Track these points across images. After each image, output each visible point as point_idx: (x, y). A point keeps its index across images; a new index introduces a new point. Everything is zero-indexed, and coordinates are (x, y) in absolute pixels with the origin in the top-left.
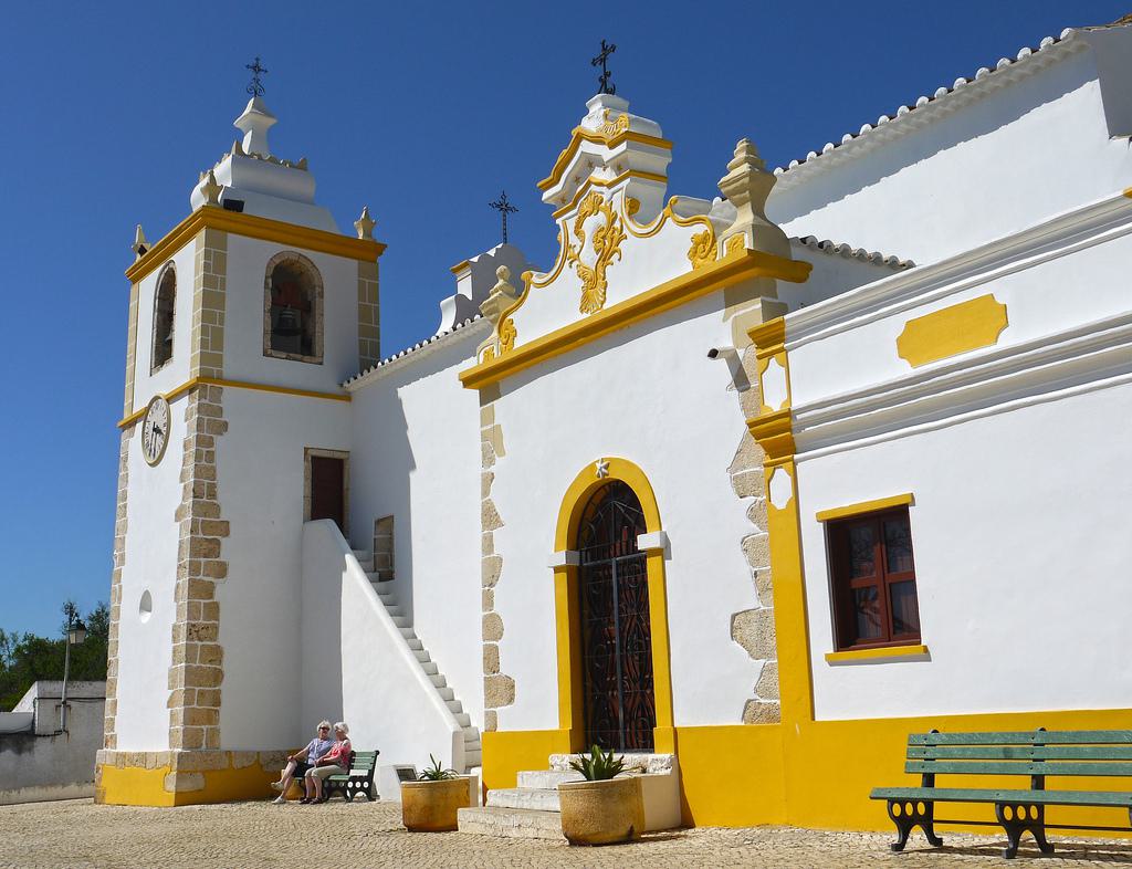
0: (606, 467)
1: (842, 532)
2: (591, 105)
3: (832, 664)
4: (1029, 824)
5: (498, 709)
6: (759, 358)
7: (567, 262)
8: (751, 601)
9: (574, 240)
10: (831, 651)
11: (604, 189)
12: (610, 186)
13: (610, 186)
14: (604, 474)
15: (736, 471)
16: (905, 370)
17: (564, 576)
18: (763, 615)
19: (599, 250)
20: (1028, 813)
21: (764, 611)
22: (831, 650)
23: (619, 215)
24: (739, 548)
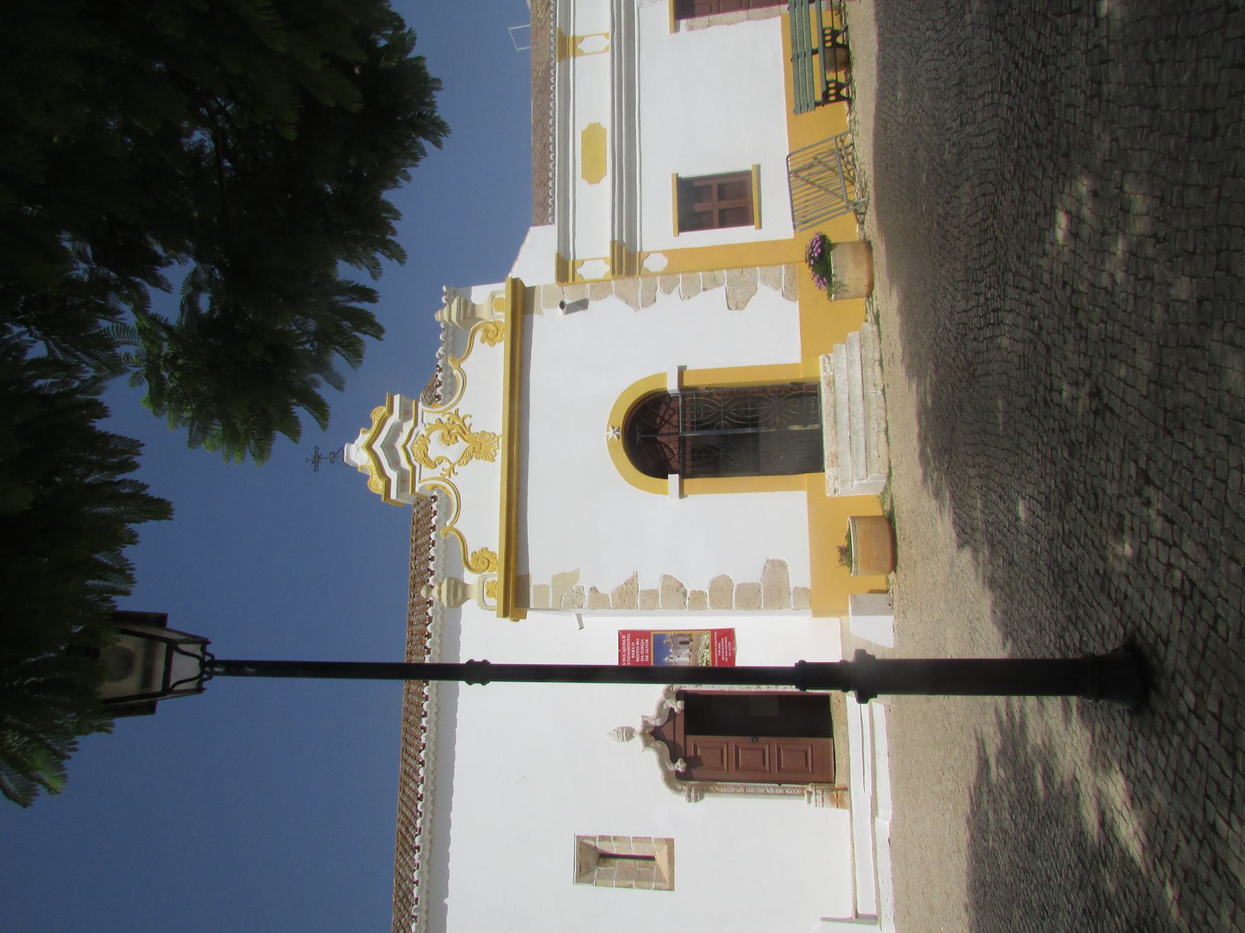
0: (613, 428)
1: (689, 220)
2: (347, 457)
3: (760, 227)
4: (833, 40)
5: (792, 585)
6: (574, 279)
7: (453, 479)
8: (719, 293)
9: (437, 472)
10: (754, 226)
11: (416, 431)
12: (416, 424)
13: (416, 424)
14: (618, 430)
15: (638, 304)
16: (607, 181)
18: (730, 282)
19: (456, 438)
20: (828, 41)
22: (753, 227)
23: (440, 416)
24: (687, 302)
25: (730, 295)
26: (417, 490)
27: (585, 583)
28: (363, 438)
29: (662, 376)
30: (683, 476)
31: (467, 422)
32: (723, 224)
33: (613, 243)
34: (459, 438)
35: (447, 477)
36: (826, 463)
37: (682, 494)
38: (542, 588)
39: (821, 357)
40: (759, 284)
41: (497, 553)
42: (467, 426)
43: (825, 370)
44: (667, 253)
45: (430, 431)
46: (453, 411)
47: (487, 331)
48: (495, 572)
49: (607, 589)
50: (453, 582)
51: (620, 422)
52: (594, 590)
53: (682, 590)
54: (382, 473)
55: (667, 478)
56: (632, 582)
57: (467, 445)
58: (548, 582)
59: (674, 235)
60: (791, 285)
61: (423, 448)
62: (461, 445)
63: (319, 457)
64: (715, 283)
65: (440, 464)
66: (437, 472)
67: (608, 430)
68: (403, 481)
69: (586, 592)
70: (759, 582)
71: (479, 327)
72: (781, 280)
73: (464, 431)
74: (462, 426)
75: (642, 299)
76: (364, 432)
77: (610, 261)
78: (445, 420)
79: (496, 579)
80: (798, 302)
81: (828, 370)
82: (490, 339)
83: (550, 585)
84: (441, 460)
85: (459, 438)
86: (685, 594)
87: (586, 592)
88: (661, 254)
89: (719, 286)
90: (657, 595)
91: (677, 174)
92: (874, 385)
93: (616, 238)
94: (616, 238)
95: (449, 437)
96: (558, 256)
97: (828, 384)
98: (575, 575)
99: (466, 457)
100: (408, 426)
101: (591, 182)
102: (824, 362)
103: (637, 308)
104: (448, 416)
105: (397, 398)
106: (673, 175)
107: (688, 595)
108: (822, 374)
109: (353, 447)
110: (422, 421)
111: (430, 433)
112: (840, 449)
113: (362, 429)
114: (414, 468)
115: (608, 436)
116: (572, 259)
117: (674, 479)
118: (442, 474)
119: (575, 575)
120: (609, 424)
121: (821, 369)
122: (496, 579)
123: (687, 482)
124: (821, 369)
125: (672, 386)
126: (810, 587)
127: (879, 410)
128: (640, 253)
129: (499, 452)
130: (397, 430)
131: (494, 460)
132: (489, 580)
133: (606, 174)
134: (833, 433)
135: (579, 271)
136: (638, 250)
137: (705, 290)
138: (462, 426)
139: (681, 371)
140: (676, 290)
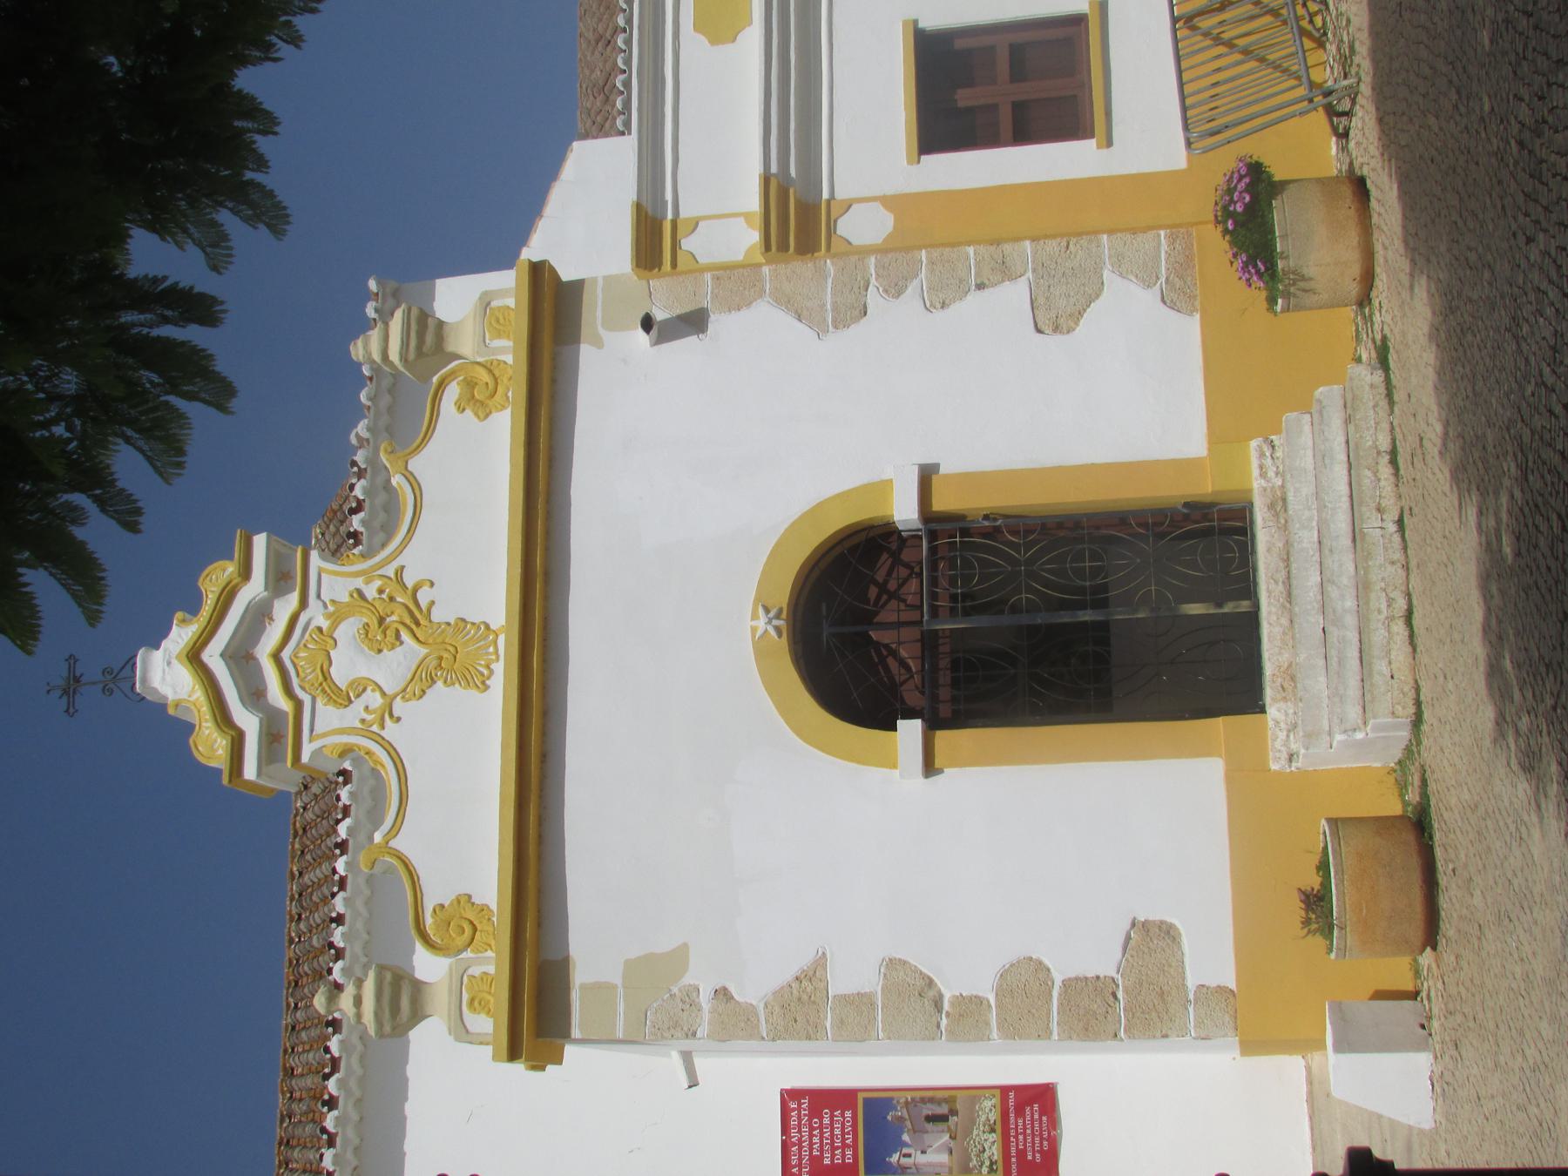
0: (767, 610)
2: (144, 680)
3: (1109, 143)
5: (1191, 983)
6: (674, 265)
7: (391, 732)
8: (1014, 296)
9: (352, 715)
10: (1094, 141)
12: (304, 603)
13: (304, 603)
14: (778, 616)
16: (752, 37)
17: (945, 739)
18: (1041, 269)
19: (398, 636)
21: (1034, 271)
22: (1092, 143)
23: (359, 582)
24: (939, 315)
25: (1041, 300)
26: (305, 758)
27: (702, 978)
28: (181, 635)
29: (882, 488)
30: (934, 724)
31: (424, 597)
32: (1022, 135)
33: (766, 180)
34: (405, 636)
35: (375, 728)
36: (1269, 693)
37: (930, 767)
38: (600, 990)
39: (1254, 444)
40: (1106, 274)
41: (494, 907)
42: (424, 605)
43: (1263, 475)
44: (891, 202)
45: (337, 619)
46: (390, 571)
47: (470, 384)
48: (490, 954)
49: (753, 990)
50: (388, 976)
51: (782, 596)
52: (722, 994)
53: (931, 993)
54: (223, 717)
55: (895, 729)
56: (813, 975)
57: (424, 651)
58: (615, 976)
59: (910, 162)
60: (1181, 277)
61: (321, 658)
62: (410, 652)
63: (77, 680)
64: (1006, 272)
65: (358, 696)
66: (352, 715)
67: (755, 616)
68: (272, 737)
69: (705, 999)
70: (1114, 974)
71: (452, 375)
72: (1159, 267)
73: (416, 618)
74: (412, 606)
75: (835, 309)
76: (184, 621)
77: (758, 221)
78: (371, 592)
79: (491, 969)
80: (1197, 316)
81: (1271, 474)
82: (478, 402)
83: (618, 981)
84: (361, 686)
85: (405, 636)
86: (938, 1004)
87: (705, 999)
88: (877, 205)
89: (1012, 277)
90: (873, 1005)
91: (916, 22)
92: (1379, 510)
93: (774, 169)
94: (774, 169)
95: (380, 635)
96: (639, 207)
97: (1271, 506)
98: (679, 958)
99: (421, 681)
100: (284, 608)
101: (715, 40)
102: (1262, 455)
103: (821, 330)
104: (378, 583)
105: (260, 542)
106: (905, 23)
107: (946, 1006)
108: (1257, 484)
109: (158, 656)
110: (319, 596)
111: (335, 626)
112: (1302, 657)
113: (179, 615)
114: (299, 705)
115: (754, 630)
116: (670, 216)
117: (910, 730)
118: (363, 721)
119: (679, 958)
120: (757, 600)
121: (1255, 472)
122: (491, 969)
123: (943, 737)
124: (1255, 472)
125: (905, 512)
126: (1232, 985)
127: (1390, 569)
128: (828, 202)
129: (499, 668)
130: (259, 616)
131: (487, 687)
132: (476, 971)
133: (750, 23)
134: (1285, 621)
135: (687, 244)
136: (825, 195)
137: (980, 287)
138: (412, 606)
139: (927, 476)
140: (912, 288)
